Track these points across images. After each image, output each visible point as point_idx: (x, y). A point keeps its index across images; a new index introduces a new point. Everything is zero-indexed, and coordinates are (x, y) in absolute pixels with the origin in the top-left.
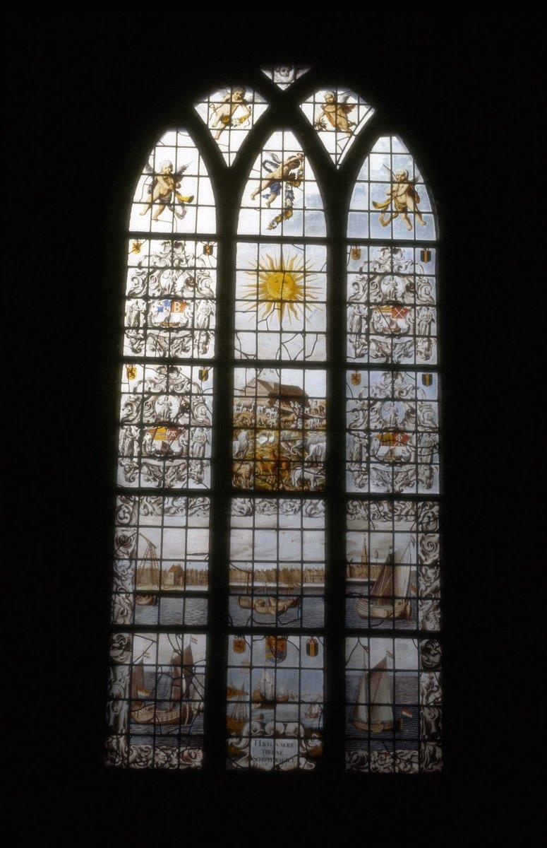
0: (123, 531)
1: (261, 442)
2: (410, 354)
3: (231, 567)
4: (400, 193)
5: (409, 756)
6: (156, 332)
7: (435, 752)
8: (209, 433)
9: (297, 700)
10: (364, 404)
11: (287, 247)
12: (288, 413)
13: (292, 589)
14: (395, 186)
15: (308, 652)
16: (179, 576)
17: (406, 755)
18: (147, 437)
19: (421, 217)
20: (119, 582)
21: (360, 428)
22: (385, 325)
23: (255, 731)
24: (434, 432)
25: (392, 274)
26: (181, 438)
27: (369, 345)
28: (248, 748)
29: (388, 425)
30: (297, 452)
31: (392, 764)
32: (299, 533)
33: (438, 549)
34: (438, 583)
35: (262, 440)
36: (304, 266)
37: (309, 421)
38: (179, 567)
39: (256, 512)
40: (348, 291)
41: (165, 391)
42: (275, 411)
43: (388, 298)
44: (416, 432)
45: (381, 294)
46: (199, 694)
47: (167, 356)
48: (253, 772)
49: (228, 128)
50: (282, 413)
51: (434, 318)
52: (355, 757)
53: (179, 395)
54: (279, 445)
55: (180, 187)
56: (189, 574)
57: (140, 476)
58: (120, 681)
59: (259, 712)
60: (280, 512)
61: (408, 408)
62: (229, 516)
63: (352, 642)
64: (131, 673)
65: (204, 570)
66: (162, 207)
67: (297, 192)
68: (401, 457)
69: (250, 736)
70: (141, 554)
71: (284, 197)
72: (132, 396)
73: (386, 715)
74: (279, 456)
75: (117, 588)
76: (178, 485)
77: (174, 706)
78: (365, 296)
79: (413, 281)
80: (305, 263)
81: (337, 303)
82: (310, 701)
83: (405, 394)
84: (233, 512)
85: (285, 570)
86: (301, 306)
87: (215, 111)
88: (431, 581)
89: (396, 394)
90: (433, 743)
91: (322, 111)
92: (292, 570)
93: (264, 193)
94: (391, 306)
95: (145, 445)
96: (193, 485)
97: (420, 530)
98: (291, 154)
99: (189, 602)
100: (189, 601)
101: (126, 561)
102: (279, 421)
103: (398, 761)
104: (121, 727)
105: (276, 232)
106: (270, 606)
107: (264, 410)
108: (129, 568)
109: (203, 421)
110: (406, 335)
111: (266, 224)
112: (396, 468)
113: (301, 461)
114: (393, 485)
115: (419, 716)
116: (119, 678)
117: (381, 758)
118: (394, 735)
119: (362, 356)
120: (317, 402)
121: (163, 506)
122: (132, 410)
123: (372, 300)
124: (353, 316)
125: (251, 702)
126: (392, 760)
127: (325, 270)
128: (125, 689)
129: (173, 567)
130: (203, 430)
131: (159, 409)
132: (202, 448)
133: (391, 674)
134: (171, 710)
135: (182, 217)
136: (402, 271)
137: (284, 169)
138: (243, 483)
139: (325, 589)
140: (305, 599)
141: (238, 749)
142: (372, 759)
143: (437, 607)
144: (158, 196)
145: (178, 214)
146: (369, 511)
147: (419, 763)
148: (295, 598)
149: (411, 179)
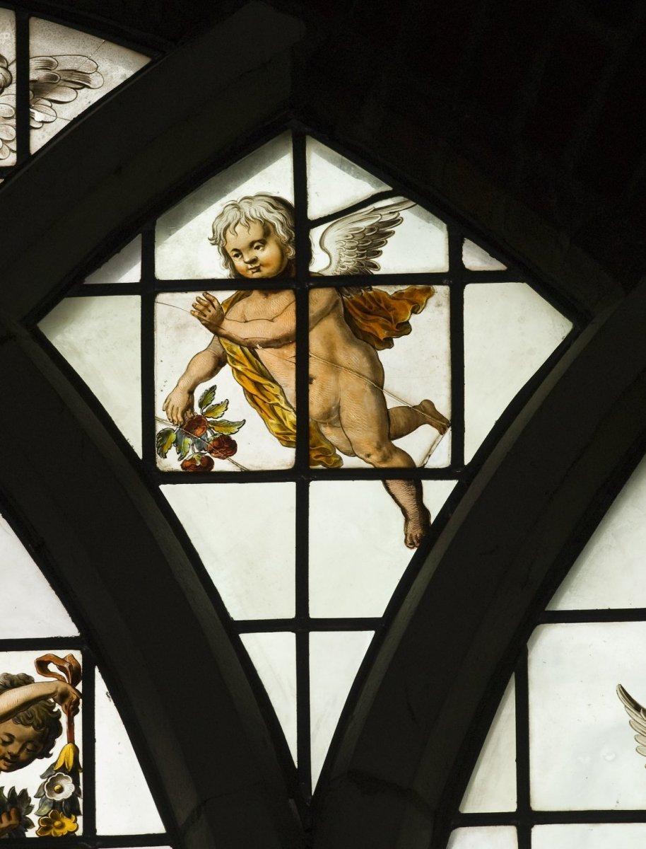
91: (204, 338)
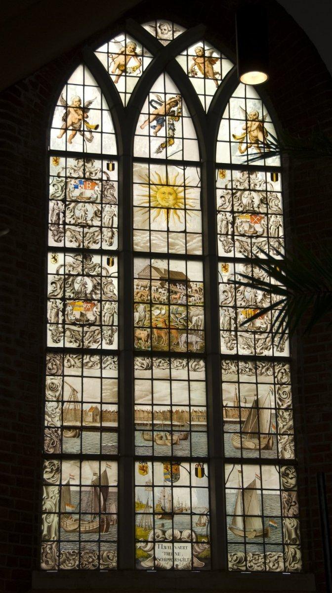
0: (52, 379)
1: (156, 314)
3: (136, 408)
4: (253, 128)
5: (276, 557)
6: (73, 227)
7: (296, 553)
8: (115, 306)
10: (231, 287)
11: (171, 168)
13: (183, 426)
14: (249, 123)
16: (97, 415)
18: (68, 309)
20: (49, 419)
22: (246, 228)
23: (158, 537)
25: (249, 190)
26: (95, 309)
27: (234, 244)
29: (250, 304)
30: (182, 321)
31: (263, 563)
32: (187, 383)
34: (291, 423)
36: (184, 182)
37: (191, 299)
38: (96, 408)
39: (154, 367)
40: (217, 203)
41: (82, 273)
42: (165, 291)
45: (242, 204)
46: (113, 508)
47: (81, 247)
49: (124, 74)
50: (169, 291)
51: (281, 223)
52: (235, 558)
53: (93, 276)
54: (169, 316)
55: (87, 117)
56: (104, 414)
57: (64, 339)
58: (52, 498)
59: (161, 522)
60: (172, 367)
63: (228, 468)
64: (60, 492)
66: (74, 132)
67: (178, 125)
68: (260, 327)
69: (154, 542)
70: (65, 399)
72: (56, 276)
73: (257, 524)
74: (169, 324)
75: (48, 424)
76: (94, 346)
77: (95, 518)
78: (230, 206)
79: (265, 196)
80: (185, 180)
81: (209, 209)
82: (199, 513)
84: (136, 367)
85: (177, 412)
86: (183, 212)
88: (286, 421)
90: (294, 546)
91: (193, 62)
92: (183, 412)
93: (152, 124)
94: (250, 214)
95: (67, 315)
96: (105, 347)
97: (276, 382)
99: (105, 436)
100: (105, 435)
101: (53, 403)
102: (168, 298)
103: (268, 561)
104: (53, 535)
105: (162, 156)
106: (167, 439)
107: (157, 289)
108: (57, 408)
109: (111, 297)
110: (260, 236)
112: (257, 336)
113: (186, 330)
115: (282, 525)
116: (50, 496)
117: (255, 558)
118: (264, 540)
119: (230, 251)
120: (196, 284)
121: (83, 360)
122: (56, 287)
123: (235, 210)
124: (222, 221)
125: (154, 514)
126: (263, 560)
127: (199, 185)
128: (55, 505)
129: (92, 408)
131: (77, 286)
132: (112, 317)
133: (259, 492)
134: (92, 522)
135: (90, 140)
136: (258, 188)
137: (167, 107)
138: (143, 345)
139: (207, 426)
140: (193, 434)
141: (145, 551)
142: (248, 559)
144: (71, 123)
145: (87, 138)
146: (238, 366)
147: (285, 562)
148: (185, 433)
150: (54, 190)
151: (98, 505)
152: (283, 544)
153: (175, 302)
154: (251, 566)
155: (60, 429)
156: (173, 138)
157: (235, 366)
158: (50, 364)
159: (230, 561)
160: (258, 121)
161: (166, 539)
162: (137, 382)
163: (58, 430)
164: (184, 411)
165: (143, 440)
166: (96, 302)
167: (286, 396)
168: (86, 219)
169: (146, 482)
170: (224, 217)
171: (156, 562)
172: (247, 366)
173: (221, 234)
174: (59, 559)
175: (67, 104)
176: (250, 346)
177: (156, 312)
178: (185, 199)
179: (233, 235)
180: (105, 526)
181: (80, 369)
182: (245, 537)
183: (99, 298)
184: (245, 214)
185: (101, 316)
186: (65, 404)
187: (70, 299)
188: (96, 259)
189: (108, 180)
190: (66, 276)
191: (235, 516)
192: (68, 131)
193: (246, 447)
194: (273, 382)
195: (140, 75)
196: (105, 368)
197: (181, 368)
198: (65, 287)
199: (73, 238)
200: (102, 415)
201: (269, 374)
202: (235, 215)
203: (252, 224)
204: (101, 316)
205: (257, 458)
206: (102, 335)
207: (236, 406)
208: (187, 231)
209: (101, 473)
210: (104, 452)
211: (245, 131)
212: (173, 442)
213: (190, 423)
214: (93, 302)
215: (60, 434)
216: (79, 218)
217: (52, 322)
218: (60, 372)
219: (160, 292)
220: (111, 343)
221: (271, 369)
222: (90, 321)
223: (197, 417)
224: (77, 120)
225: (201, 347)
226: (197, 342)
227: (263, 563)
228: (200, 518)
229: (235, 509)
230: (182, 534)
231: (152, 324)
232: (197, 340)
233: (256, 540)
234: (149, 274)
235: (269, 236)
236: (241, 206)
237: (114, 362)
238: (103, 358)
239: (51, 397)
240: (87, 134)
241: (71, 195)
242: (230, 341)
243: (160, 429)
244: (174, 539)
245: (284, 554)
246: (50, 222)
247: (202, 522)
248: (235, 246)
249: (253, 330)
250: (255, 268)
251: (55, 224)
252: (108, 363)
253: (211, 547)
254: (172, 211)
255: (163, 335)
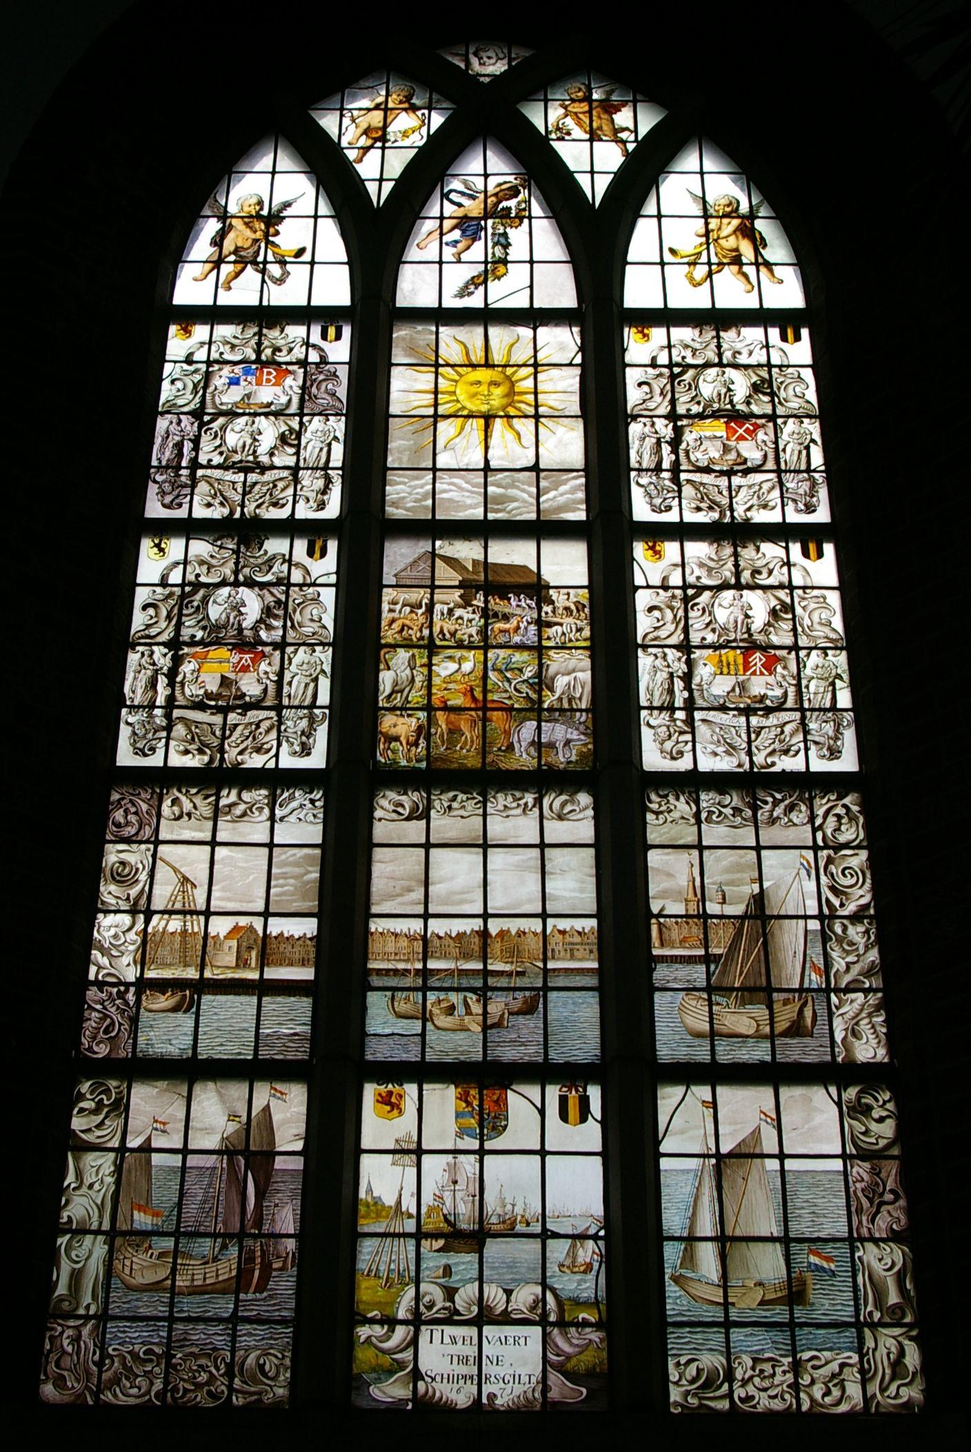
1: (444, 673)
2: (772, 504)
3: (373, 928)
4: (724, 233)
5: (834, 1366)
6: (217, 473)
7: (902, 1352)
8: (325, 656)
9: (537, 1228)
10: (674, 597)
12: (506, 617)
13: (519, 974)
15: (564, 1116)
16: (250, 948)
17: (827, 1363)
18: (187, 668)
19: (771, 271)
20: (104, 961)
21: (670, 641)
22: (715, 454)
23: (429, 1308)
24: (836, 648)
26: (263, 666)
27: (680, 491)
28: (411, 1351)
30: (524, 688)
31: (788, 1386)
32: (537, 852)
33: (868, 881)
34: (873, 955)
35: (444, 668)
36: (535, 356)
37: (551, 632)
38: (251, 929)
39: (433, 813)
40: (629, 397)
41: (232, 579)
42: (474, 612)
43: (716, 406)
44: (795, 648)
46: (286, 1219)
47: (237, 515)
48: (428, 1412)
49: (379, 144)
50: (485, 613)
52: (692, 1371)
53: (262, 586)
54: (485, 677)
55: (277, 233)
58: (91, 1186)
59: (443, 1260)
60: (489, 810)
61: (774, 602)
62: (370, 819)
64: (118, 1169)
65: (309, 936)
66: (239, 267)
67: (518, 236)
68: (763, 698)
69: (417, 1321)
70: (157, 904)
71: (490, 244)
72: (159, 590)
73: (768, 1265)
76: (255, 761)
79: (767, 376)
80: (536, 351)
83: (765, 575)
84: (378, 813)
85: (503, 934)
87: (353, 121)
88: (858, 951)
89: (746, 576)
90: (897, 1331)
92: (521, 933)
94: (722, 420)
95: (182, 684)
96: (288, 761)
97: (820, 843)
98: (501, 179)
99: (273, 1006)
101: (119, 916)
102: (483, 632)
103: (806, 1380)
104: (87, 1299)
105: (475, 301)
107: (451, 611)
108: (130, 929)
109: (314, 634)
110: (757, 469)
111: (451, 288)
112: (754, 721)
113: (536, 710)
114: (750, 753)
116: (87, 1182)
117: (762, 1371)
118: (792, 1313)
119: (669, 508)
120: (568, 594)
121: (217, 800)
124: (643, 439)
125: (419, 1235)
126: (790, 1377)
127: (578, 360)
128: (101, 1208)
129: (236, 928)
130: (314, 651)
133: (773, 1164)
134: (215, 1259)
136: (743, 359)
137: (489, 201)
139: (599, 972)
140: (552, 995)
142: (739, 1374)
143: (878, 1008)
144: (232, 248)
145: (272, 278)
148: (527, 994)
149: (744, 208)
150: (174, 392)
151: (238, 1210)
152: (858, 1326)
153: (502, 639)
154: (749, 1398)
155: (132, 989)
156: (505, 262)
157: (687, 803)
158: (121, 811)
159: (676, 1383)
160: (738, 217)
161: (457, 1313)
162: (378, 853)
163: (127, 991)
164: (524, 933)
165: (391, 1018)
166: (268, 649)
167: (855, 879)
168: (255, 452)
169: (397, 1141)
170: (647, 430)
171: (421, 1386)
172: (727, 800)
173: (639, 470)
174: (100, 1373)
175: (226, 211)
176: (734, 748)
177: (446, 668)
178: (536, 393)
179: (676, 469)
180: (257, 1273)
181: (210, 824)
182: (726, 1305)
183: (278, 639)
184: (708, 421)
185: (279, 683)
186: (156, 918)
187: (193, 643)
188: (276, 546)
189: (324, 360)
190: (187, 589)
191: (691, 1240)
192: (223, 266)
193: (724, 1030)
194: (810, 844)
195: (421, 143)
196: (282, 819)
197: (519, 811)
198: (180, 615)
199: (214, 497)
200: (267, 949)
201: (795, 820)
202: (679, 423)
203: (732, 443)
204: (279, 683)
205: (763, 1063)
206: (279, 731)
207: (691, 912)
208: (542, 466)
209: (254, 1114)
210: (264, 1053)
211: (704, 239)
212: (489, 1022)
213: (545, 964)
214: (260, 648)
215: (132, 1003)
216: (236, 452)
217: (136, 703)
218: (147, 832)
219: (461, 618)
220: (306, 750)
221: (803, 808)
222: (247, 699)
223: (568, 947)
224: (250, 242)
225: (580, 754)
226: (568, 743)
227: (788, 1386)
228: (573, 1246)
229: (693, 1218)
230: (513, 1297)
231: (433, 697)
232: (569, 736)
233: (764, 1314)
234: (429, 574)
235: (783, 467)
236: (699, 403)
237: (312, 802)
238: (279, 792)
239: (113, 901)
240: (275, 270)
241: (218, 401)
242: (670, 736)
243: (445, 985)
244: (485, 1312)
245: (861, 1356)
246: (154, 463)
247: (580, 1260)
248: (683, 495)
249: (742, 706)
250: (745, 547)
251: (167, 467)
252: (295, 804)
253: (610, 1340)
254: (498, 424)
255: (465, 727)
